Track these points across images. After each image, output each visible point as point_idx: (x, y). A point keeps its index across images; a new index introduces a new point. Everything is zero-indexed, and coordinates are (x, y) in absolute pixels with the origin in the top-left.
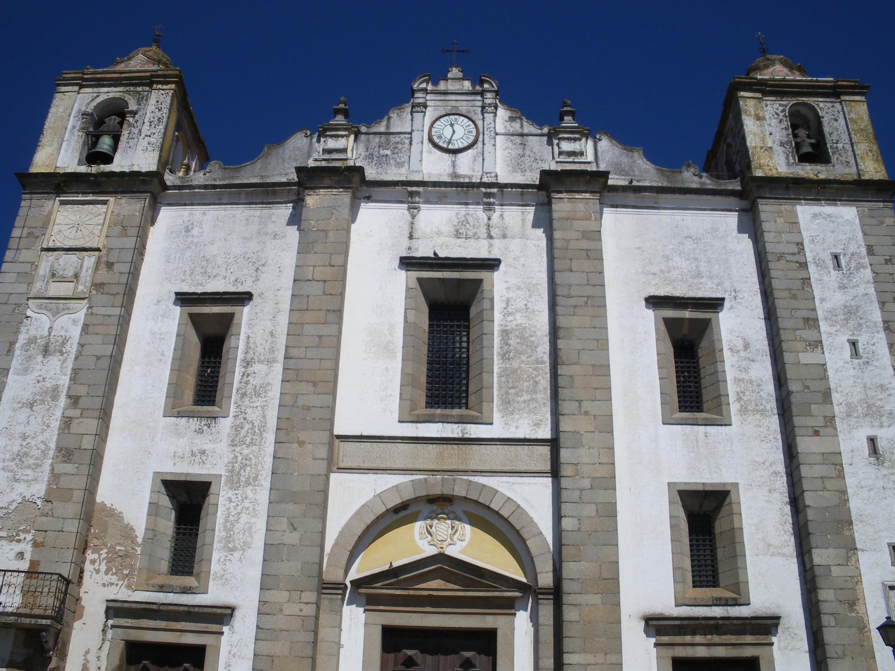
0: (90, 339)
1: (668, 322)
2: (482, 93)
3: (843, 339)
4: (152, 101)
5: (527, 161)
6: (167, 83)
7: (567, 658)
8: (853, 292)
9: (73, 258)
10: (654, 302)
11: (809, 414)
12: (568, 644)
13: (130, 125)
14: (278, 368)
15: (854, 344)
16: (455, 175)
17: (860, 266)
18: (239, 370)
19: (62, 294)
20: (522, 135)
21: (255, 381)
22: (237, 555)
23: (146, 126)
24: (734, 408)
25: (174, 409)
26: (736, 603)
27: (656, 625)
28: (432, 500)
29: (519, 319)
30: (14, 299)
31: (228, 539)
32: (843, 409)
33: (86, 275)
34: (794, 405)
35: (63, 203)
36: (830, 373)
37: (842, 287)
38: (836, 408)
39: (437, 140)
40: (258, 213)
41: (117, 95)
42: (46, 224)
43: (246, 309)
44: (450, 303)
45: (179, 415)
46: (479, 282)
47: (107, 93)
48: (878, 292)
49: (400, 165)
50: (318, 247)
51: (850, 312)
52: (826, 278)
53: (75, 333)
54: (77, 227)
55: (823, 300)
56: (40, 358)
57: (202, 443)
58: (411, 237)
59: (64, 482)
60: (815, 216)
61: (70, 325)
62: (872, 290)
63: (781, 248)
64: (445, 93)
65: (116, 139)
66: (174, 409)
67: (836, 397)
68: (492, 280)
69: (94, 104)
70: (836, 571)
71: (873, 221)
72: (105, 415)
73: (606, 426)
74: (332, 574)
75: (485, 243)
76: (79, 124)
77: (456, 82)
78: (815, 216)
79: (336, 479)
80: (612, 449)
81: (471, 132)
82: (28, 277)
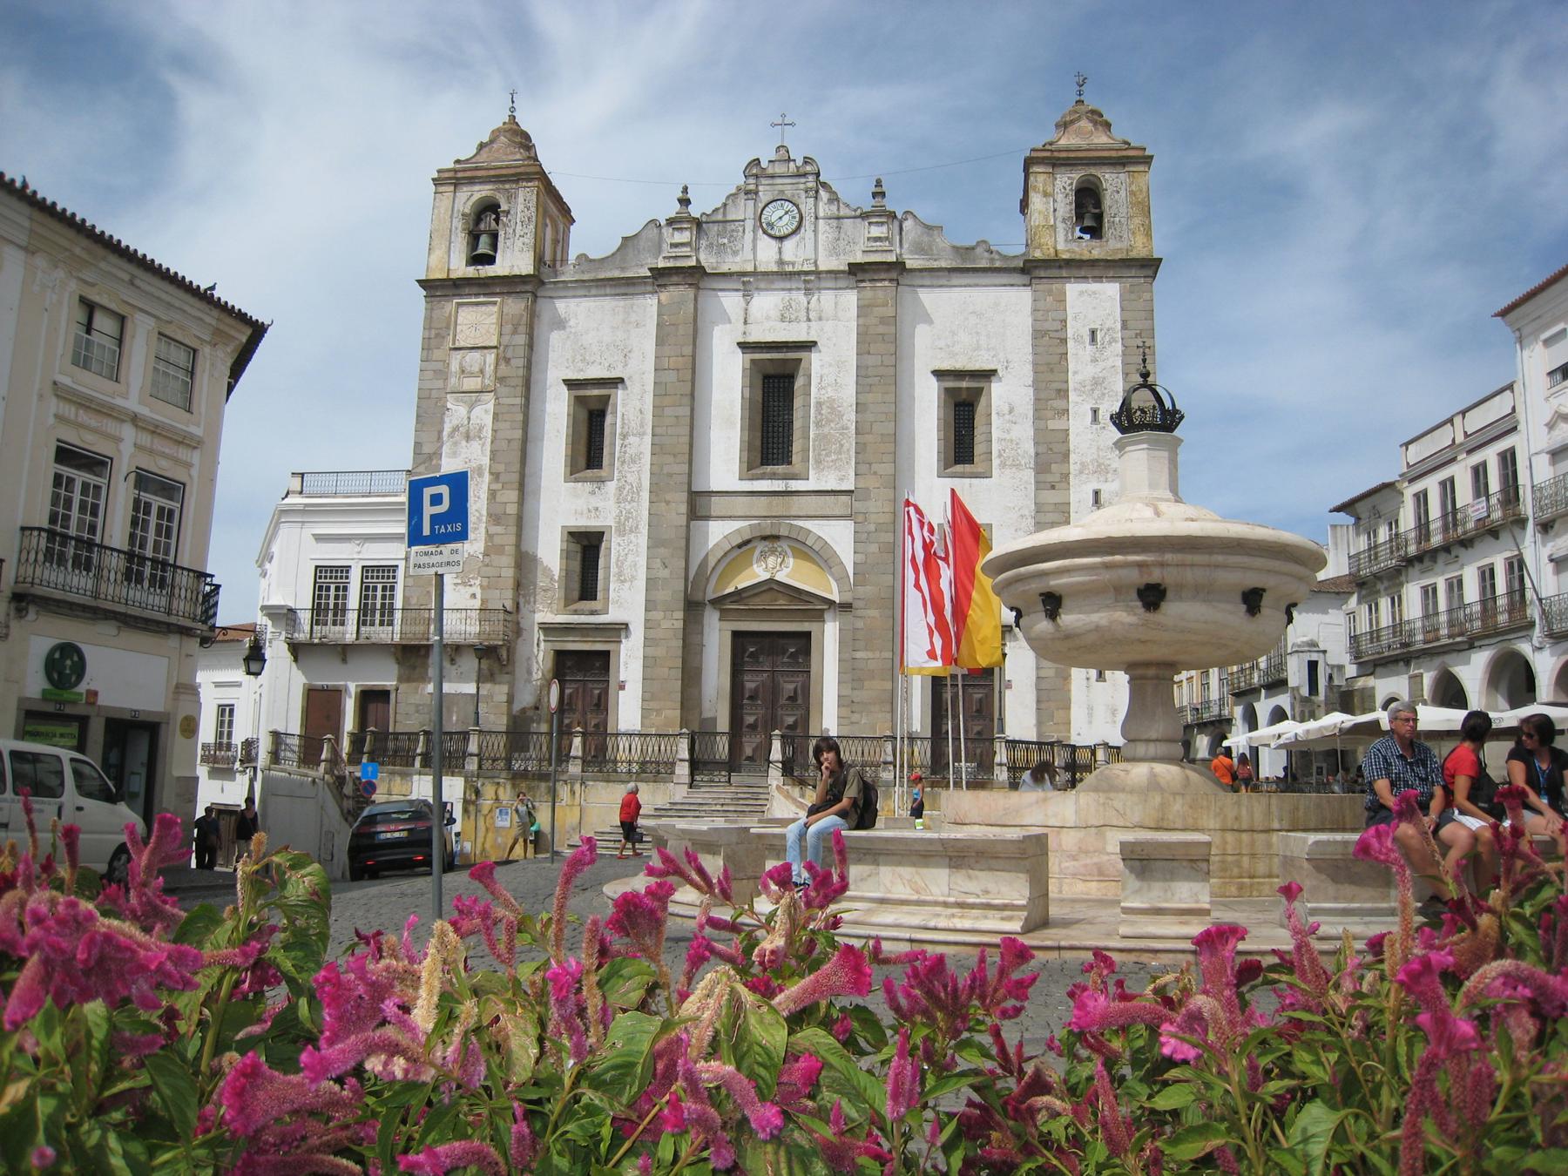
0: (501, 425)
1: (947, 390)
4: (521, 199)
5: (842, 243)
6: (530, 180)
8: (1101, 365)
9: (476, 355)
10: (939, 374)
13: (505, 225)
14: (648, 439)
15: (1095, 412)
16: (781, 262)
17: (1113, 340)
19: (472, 388)
20: (838, 218)
21: (631, 451)
22: (627, 585)
23: (519, 227)
29: (830, 393)
31: (620, 574)
32: (1078, 467)
33: (489, 369)
35: (459, 304)
36: (1071, 437)
37: (1094, 360)
38: (1072, 467)
40: (622, 303)
41: (489, 193)
42: (450, 325)
43: (620, 392)
44: (776, 381)
45: (576, 481)
46: (800, 360)
47: (481, 192)
48: (1125, 364)
49: (735, 253)
51: (1097, 382)
52: (1081, 352)
53: (488, 420)
54: (475, 326)
55: (1075, 373)
56: (464, 443)
57: (595, 501)
58: (745, 322)
59: (497, 540)
60: (1081, 293)
61: (483, 415)
62: (1119, 363)
64: (773, 177)
67: (1072, 456)
69: (470, 203)
71: (1133, 296)
75: (804, 325)
76: (460, 226)
78: (1081, 293)
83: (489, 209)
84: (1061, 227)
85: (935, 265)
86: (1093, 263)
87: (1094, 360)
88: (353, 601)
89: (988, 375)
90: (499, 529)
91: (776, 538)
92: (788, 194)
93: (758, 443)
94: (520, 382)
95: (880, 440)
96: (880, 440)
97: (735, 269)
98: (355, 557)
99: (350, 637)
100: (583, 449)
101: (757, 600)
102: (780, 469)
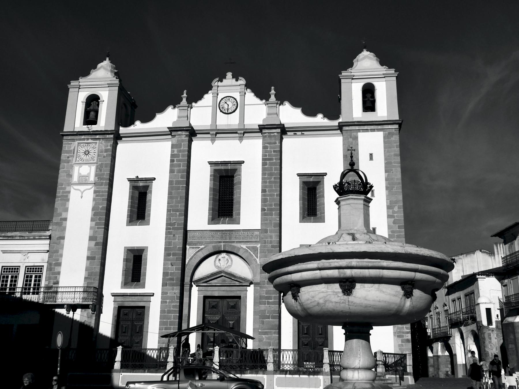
10: (299, 175)
39: (222, 109)
68: (240, 169)
77: (229, 79)
81: (234, 105)
82: (70, 176)
93: (217, 208)
95: (272, 206)
96: (272, 206)
101: (215, 281)
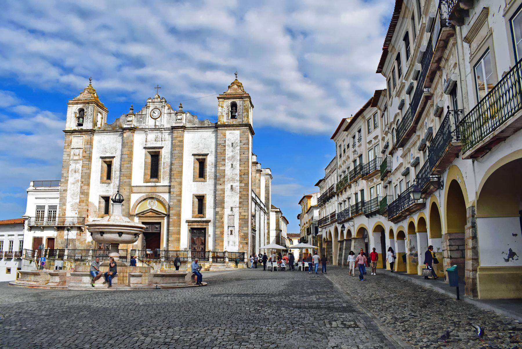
0: (84, 169)
2: (162, 102)
3: (230, 164)
7: (170, 228)
9: (78, 150)
11: (219, 180)
12: (170, 226)
15: (232, 165)
18: (114, 173)
20: (170, 113)
24: (208, 178)
25: (102, 182)
26: (203, 217)
27: (188, 222)
28: (150, 198)
30: (67, 161)
33: (81, 155)
34: (218, 178)
37: (233, 151)
44: (155, 156)
50: (127, 147)
51: (233, 157)
53: (80, 168)
59: (82, 199)
61: (79, 166)
62: (239, 152)
63: (221, 142)
65: (83, 118)
66: (102, 182)
70: (220, 212)
72: (88, 185)
73: (180, 184)
74: (131, 213)
79: (132, 195)
80: (181, 189)
82: (69, 155)
83: (81, 111)
84: (225, 116)
85: (194, 126)
86: (233, 126)
87: (233, 151)
88: (46, 214)
89: (207, 155)
90: (83, 196)
91: (152, 198)
92: (158, 107)
94: (88, 157)
97: (144, 127)
98: (47, 203)
99: (45, 224)
100: (105, 175)
102: (154, 180)
